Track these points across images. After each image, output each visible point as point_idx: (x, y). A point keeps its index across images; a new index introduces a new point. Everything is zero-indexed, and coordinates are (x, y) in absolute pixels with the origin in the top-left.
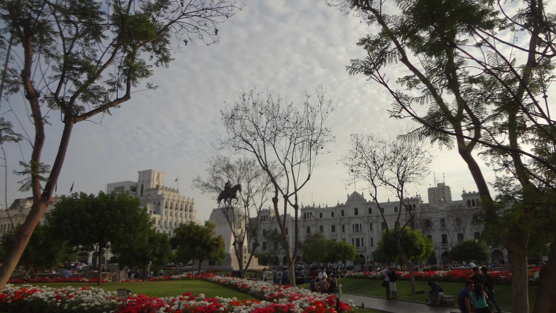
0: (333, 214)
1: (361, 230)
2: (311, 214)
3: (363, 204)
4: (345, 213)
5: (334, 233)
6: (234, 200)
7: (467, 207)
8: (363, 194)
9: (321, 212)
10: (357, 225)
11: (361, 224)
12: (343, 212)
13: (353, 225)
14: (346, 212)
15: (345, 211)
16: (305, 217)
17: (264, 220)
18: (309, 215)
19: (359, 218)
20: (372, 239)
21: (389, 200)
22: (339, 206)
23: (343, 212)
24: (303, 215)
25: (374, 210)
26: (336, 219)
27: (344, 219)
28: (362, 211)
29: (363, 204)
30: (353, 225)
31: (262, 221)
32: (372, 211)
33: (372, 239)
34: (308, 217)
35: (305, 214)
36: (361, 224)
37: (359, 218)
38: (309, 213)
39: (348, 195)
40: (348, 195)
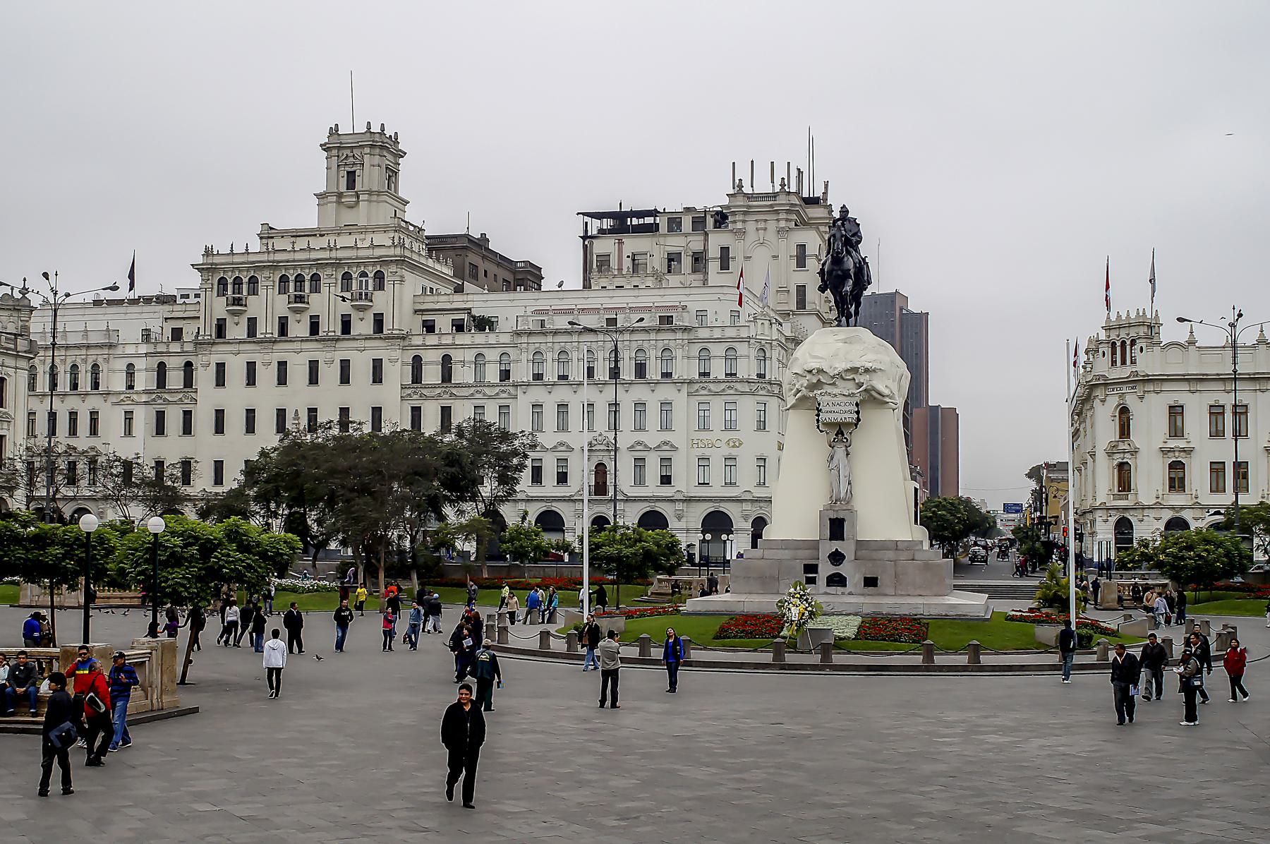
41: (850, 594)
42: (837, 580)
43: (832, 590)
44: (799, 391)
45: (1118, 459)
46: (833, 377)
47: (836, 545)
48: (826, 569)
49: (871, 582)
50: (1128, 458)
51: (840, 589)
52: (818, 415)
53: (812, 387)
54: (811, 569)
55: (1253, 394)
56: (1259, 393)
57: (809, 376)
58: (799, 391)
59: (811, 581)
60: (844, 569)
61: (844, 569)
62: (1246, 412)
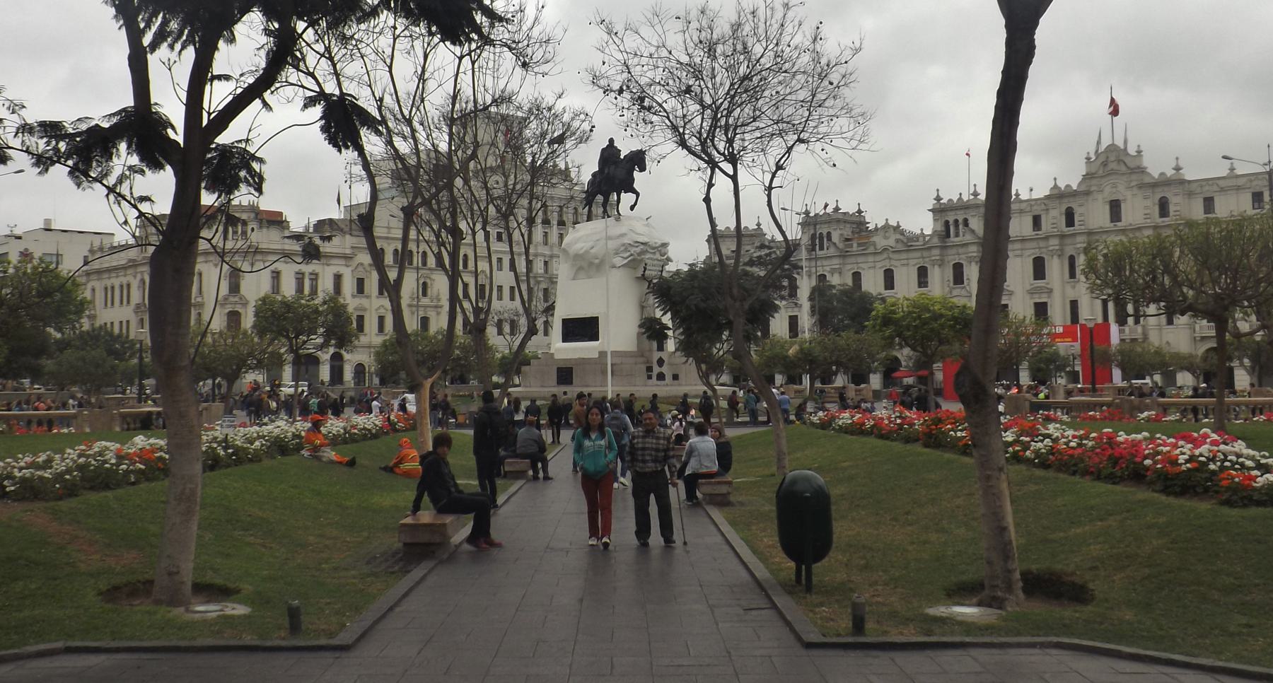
0: (1037, 222)
2: (966, 222)
4: (1077, 218)
5: (1040, 283)
6: (627, 198)
8: (1139, 152)
14: (1081, 215)
15: (1078, 211)
16: (948, 235)
17: (821, 248)
18: (961, 227)
22: (1058, 195)
24: (940, 227)
25: (1176, 204)
26: (1047, 238)
27: (1074, 235)
29: (1141, 186)
31: (814, 249)
32: (1172, 208)
35: (947, 224)
38: (961, 221)
39: (1088, 159)
41: (667, 385)
42: (661, 377)
43: (659, 383)
44: (632, 255)
45: (228, 309)
46: (654, 248)
47: (660, 354)
48: (656, 370)
49: (675, 377)
50: (238, 308)
51: (663, 382)
52: (644, 272)
53: (643, 252)
54: (650, 369)
55: (321, 266)
56: (326, 267)
57: (642, 247)
58: (632, 255)
59: (650, 377)
60: (665, 369)
61: (665, 369)
62: (316, 279)
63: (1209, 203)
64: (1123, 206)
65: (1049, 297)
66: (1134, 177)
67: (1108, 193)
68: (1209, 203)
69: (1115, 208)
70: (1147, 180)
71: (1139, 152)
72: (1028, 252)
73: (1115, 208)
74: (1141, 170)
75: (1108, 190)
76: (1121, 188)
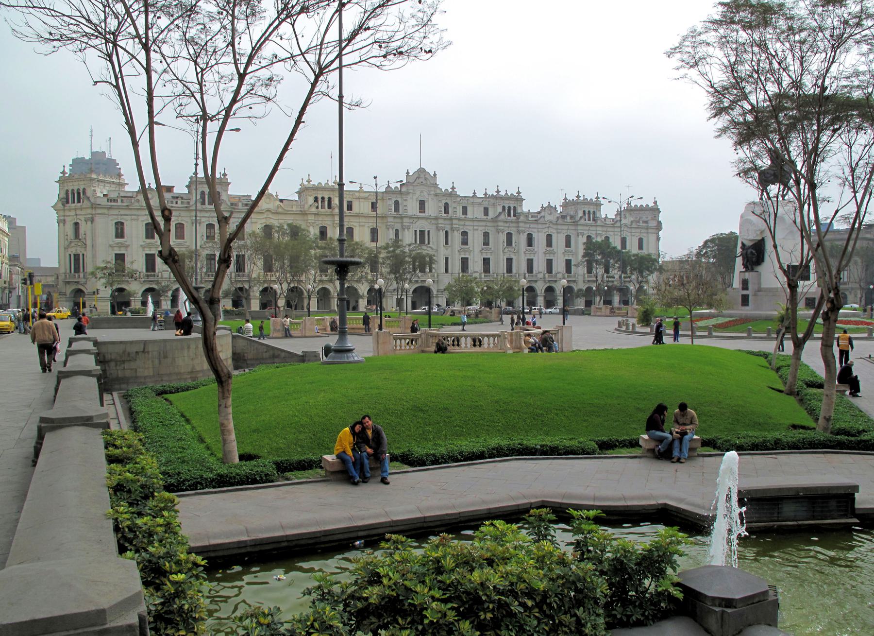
0: (374, 206)
1: (429, 243)
3: (436, 195)
7: (314, 210)
8: (435, 175)
9: (350, 200)
10: (422, 233)
11: (429, 231)
12: (397, 204)
13: (416, 231)
19: (427, 219)
20: (447, 259)
21: (475, 193)
23: (397, 204)
26: (383, 217)
28: (432, 209)
29: (436, 195)
30: (416, 231)
33: (447, 259)
34: (323, 207)
36: (429, 231)
37: (427, 219)
39: (408, 173)
40: (408, 173)
63: (465, 211)
64: (426, 204)
65: (126, 250)
66: (433, 189)
67: (418, 196)
68: (465, 211)
69: (422, 204)
70: (438, 191)
71: (435, 175)
72: (371, 224)
73: (422, 204)
74: (435, 185)
75: (418, 193)
76: (425, 194)
